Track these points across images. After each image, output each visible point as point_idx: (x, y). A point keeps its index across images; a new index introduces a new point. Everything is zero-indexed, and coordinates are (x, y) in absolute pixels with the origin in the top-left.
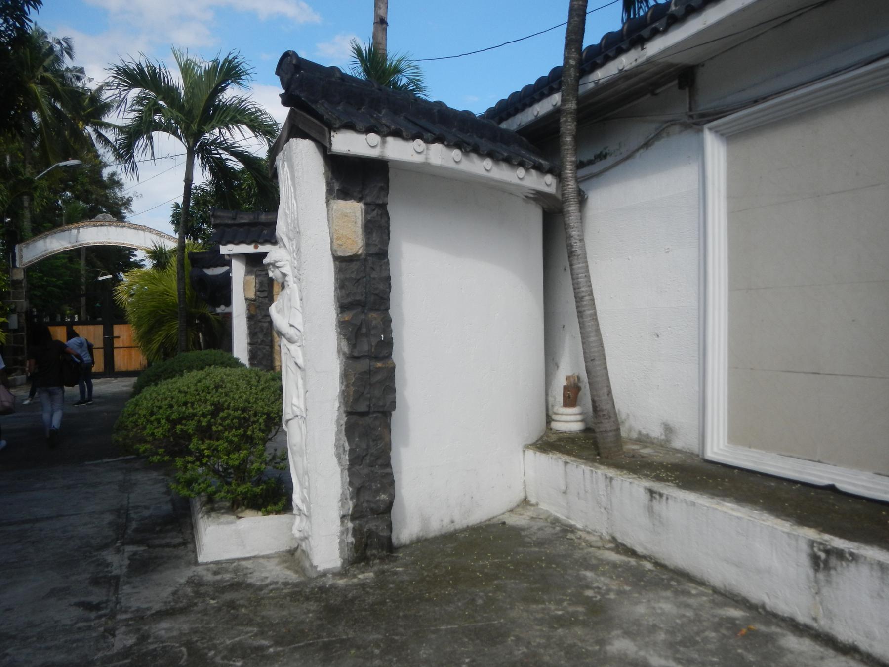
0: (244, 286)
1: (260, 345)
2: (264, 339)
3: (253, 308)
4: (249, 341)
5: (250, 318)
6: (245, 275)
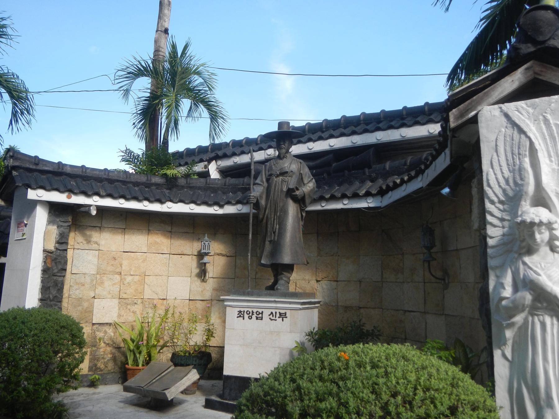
0: (44, 236)
1: (51, 301)
2: (57, 295)
3: (49, 261)
4: (40, 296)
5: (45, 271)
6: (47, 225)
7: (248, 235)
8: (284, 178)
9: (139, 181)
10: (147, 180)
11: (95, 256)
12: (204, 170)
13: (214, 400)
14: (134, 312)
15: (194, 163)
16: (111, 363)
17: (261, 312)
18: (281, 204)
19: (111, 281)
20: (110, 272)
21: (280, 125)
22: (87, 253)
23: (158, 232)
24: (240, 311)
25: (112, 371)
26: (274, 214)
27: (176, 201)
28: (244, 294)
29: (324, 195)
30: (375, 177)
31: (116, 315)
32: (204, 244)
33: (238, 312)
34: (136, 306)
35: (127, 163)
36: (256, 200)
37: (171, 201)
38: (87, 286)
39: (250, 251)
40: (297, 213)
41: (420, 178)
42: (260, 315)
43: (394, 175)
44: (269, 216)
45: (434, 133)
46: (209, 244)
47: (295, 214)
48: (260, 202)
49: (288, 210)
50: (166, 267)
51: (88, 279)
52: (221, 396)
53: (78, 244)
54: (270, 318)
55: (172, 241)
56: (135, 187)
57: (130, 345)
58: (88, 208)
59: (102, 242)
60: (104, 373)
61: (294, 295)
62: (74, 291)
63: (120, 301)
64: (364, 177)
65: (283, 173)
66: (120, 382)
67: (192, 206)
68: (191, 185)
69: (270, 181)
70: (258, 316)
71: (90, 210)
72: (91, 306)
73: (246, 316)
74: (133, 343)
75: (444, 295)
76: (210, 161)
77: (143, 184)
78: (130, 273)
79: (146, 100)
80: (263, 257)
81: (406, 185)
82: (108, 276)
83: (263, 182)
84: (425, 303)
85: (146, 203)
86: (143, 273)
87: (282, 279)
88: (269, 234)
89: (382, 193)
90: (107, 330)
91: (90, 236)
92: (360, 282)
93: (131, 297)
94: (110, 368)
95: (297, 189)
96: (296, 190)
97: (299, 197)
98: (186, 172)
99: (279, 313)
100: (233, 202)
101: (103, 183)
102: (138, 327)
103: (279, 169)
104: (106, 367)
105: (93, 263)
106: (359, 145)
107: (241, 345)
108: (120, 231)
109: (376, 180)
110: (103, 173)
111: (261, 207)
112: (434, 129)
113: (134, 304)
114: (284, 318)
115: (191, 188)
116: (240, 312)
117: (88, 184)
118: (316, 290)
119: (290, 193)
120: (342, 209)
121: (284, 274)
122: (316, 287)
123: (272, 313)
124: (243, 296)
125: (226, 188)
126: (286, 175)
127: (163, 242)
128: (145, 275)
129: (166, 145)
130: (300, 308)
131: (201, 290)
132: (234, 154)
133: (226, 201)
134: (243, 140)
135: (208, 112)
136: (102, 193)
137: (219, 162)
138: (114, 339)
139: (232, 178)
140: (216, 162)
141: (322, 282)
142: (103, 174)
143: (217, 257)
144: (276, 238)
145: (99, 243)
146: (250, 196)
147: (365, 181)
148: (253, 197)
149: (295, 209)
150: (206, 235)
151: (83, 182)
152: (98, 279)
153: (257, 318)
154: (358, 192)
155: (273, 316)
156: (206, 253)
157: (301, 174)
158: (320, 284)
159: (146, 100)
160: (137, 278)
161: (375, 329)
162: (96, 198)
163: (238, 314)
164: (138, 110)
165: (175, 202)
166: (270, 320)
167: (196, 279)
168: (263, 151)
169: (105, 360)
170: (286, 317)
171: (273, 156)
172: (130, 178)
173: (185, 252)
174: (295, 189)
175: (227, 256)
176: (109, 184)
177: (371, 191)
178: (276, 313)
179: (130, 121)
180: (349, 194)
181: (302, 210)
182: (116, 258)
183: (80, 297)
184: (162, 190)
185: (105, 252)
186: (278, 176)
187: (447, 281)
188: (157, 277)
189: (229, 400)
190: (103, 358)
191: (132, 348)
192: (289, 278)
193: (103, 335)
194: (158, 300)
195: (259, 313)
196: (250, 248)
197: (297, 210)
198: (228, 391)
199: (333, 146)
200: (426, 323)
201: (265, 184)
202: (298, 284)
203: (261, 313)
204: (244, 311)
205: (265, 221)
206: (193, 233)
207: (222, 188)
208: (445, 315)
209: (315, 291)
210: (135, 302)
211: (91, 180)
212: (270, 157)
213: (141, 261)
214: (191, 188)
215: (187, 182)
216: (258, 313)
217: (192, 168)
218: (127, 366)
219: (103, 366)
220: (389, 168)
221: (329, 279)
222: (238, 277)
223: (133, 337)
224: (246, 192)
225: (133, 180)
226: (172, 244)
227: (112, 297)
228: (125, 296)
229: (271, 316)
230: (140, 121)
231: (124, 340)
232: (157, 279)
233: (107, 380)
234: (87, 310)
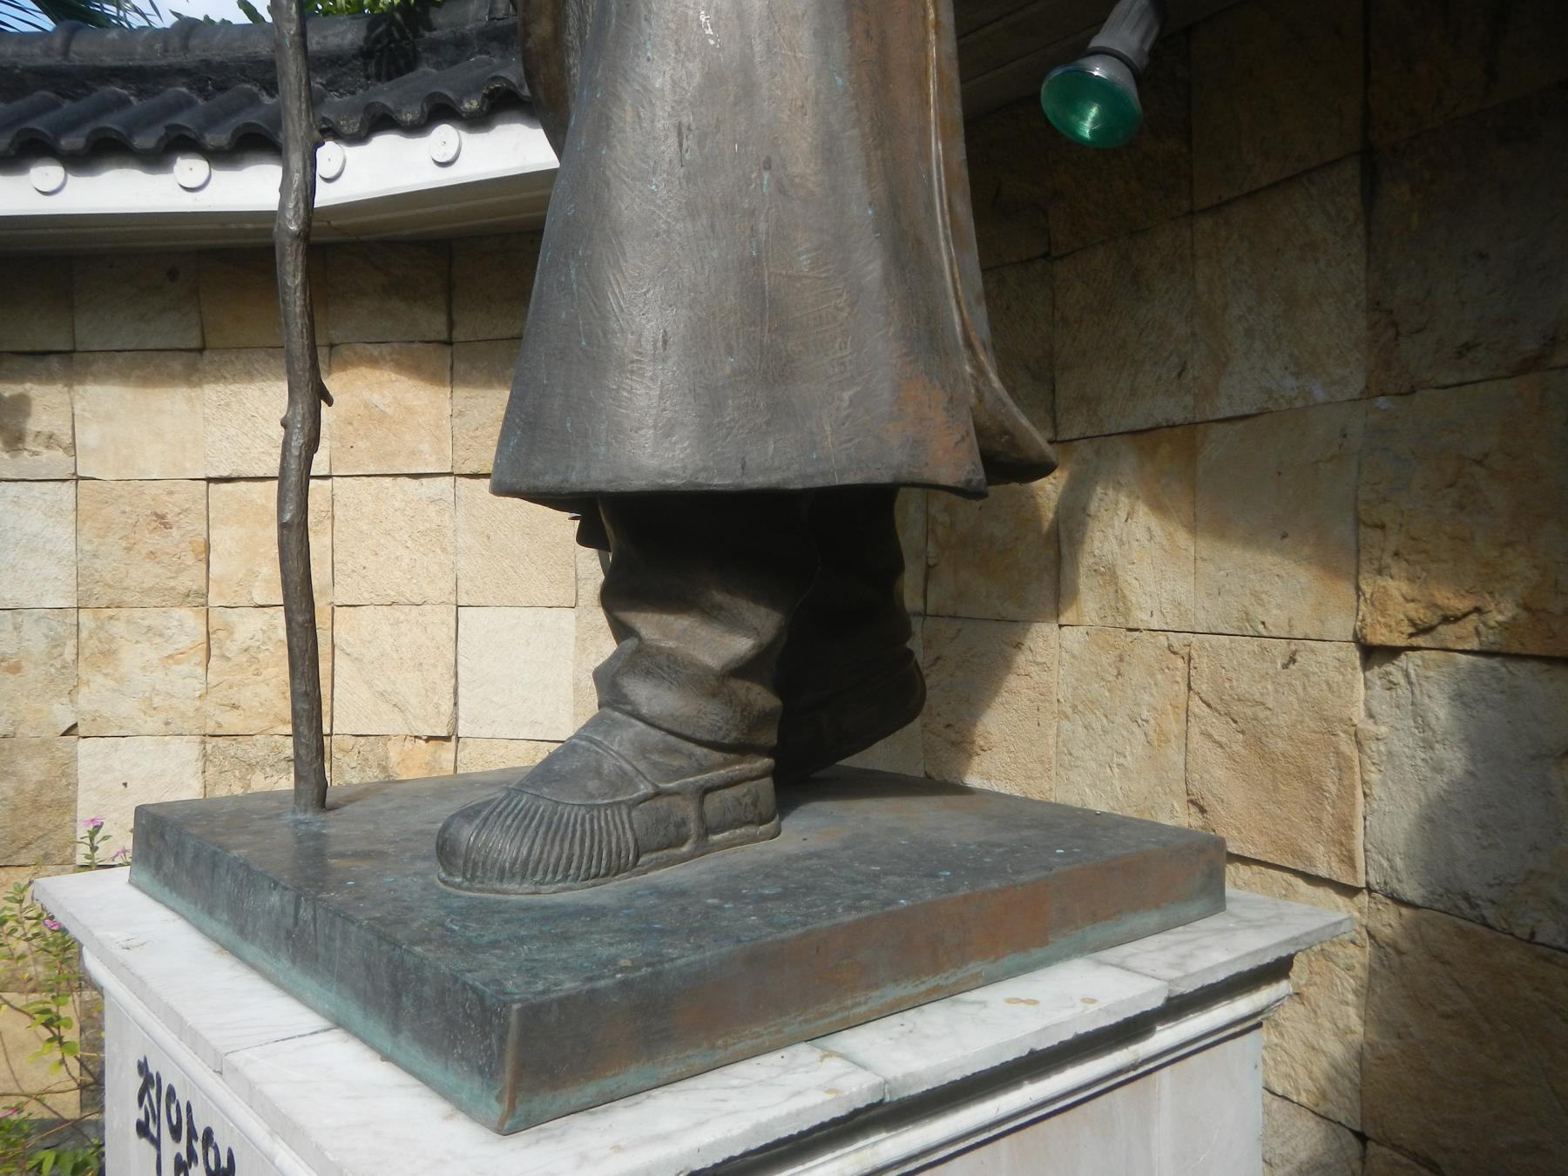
19: (157, 640)
22: (16, 501)
23: (375, 350)
38: (30, 672)
50: (444, 550)
51: (35, 639)
55: (462, 393)
67: (445, 136)
72: (64, 774)
82: (138, 613)
93: (265, 724)
108: (177, 365)
122: (1358, 715)
127: (410, 410)
141: (1409, 661)
152: (84, 635)
158: (1391, 686)
182: (170, 518)
185: (105, 484)
188: (397, 613)
194: (408, 745)
202: (1202, 663)
221: (1490, 638)
227: (163, 729)
228: (232, 722)
232: (398, 622)
234: (45, 799)
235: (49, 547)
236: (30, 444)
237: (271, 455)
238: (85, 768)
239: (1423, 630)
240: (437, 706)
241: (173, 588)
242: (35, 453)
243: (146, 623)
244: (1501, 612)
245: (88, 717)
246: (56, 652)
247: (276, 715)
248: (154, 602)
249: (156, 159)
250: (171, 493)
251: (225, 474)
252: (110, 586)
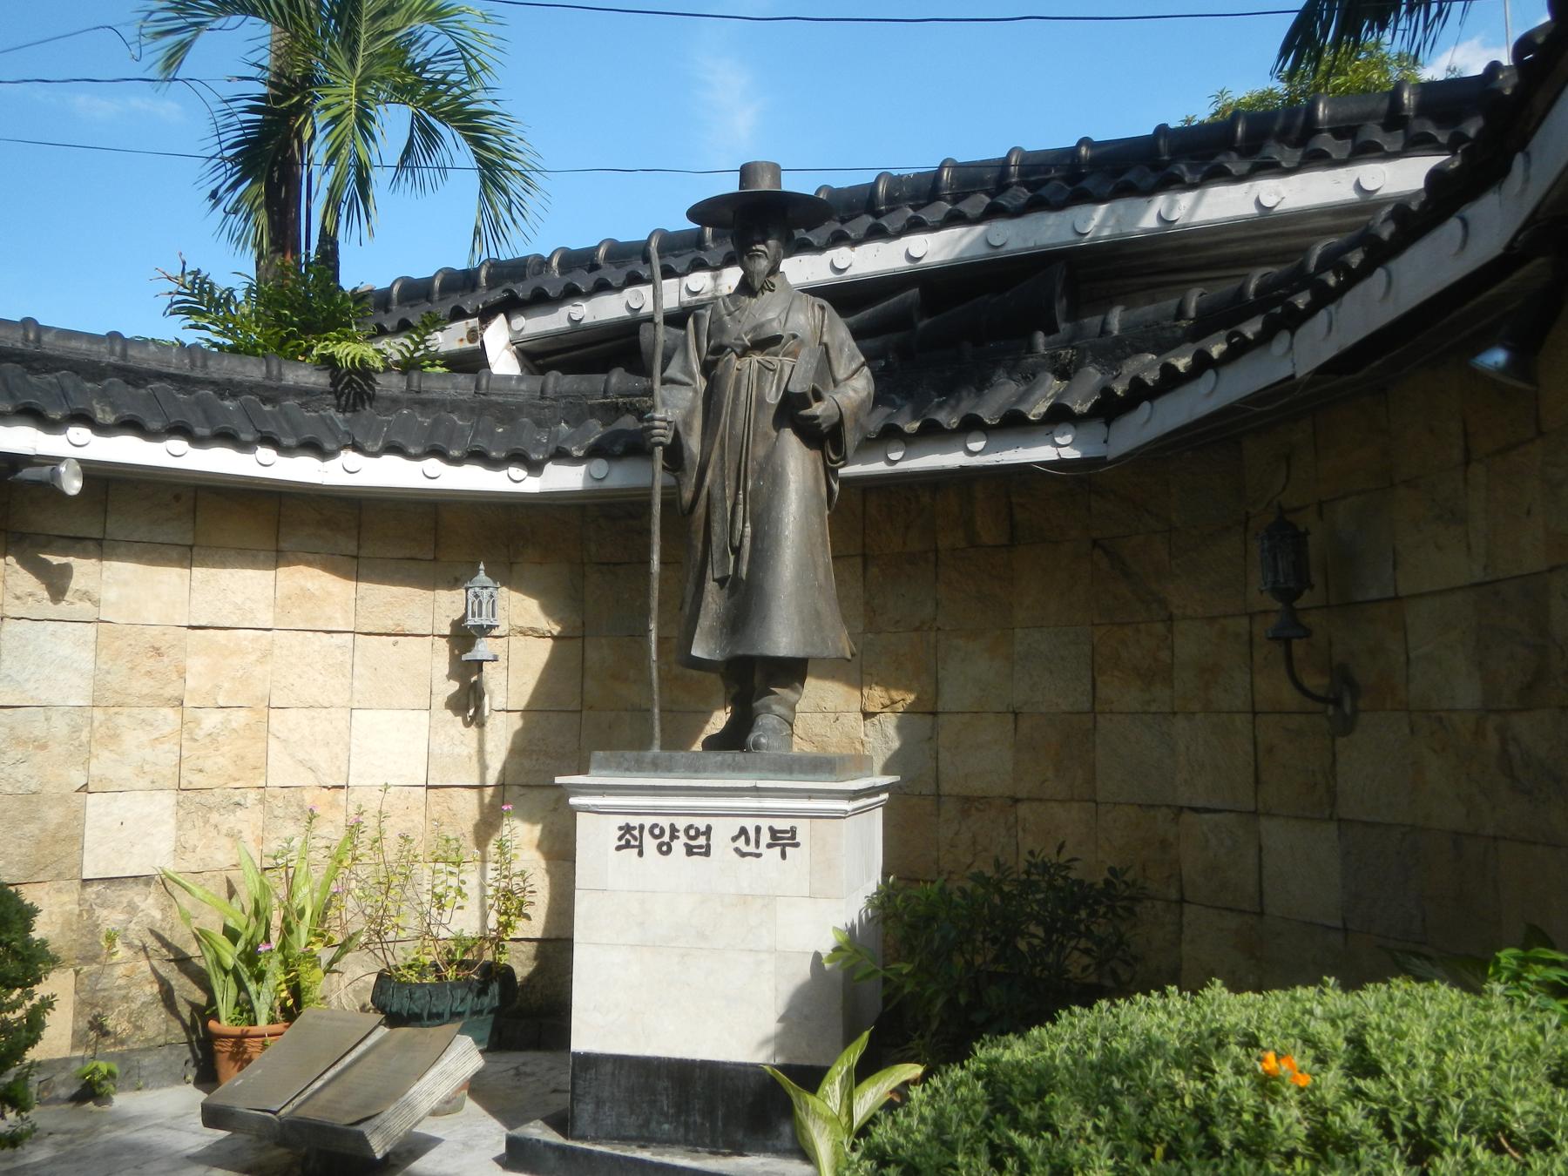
7: (647, 562)
8: (768, 358)
9: (238, 378)
10: (268, 376)
11: (85, 643)
12: (467, 345)
13: (538, 1141)
14: (234, 836)
15: (436, 323)
16: (156, 1012)
17: (703, 829)
18: (760, 451)
20: (142, 697)
21: (746, 172)
22: (53, 634)
23: (310, 557)
24: (627, 825)
25: (161, 1040)
26: (733, 484)
27: (376, 449)
28: (639, 767)
29: (899, 423)
30: (1071, 361)
31: (167, 846)
32: (477, 596)
33: (621, 828)
34: (239, 813)
35: (192, 322)
36: (671, 434)
37: (357, 448)
39: (654, 614)
40: (817, 480)
41: (1281, 343)
42: (702, 840)
43: (1143, 351)
44: (717, 493)
45: (1276, 209)
46: (492, 596)
47: (810, 483)
48: (684, 442)
49: (784, 468)
50: (344, 676)
51: (60, 726)
52: (561, 1123)
53: (17, 602)
54: (737, 850)
55: (363, 586)
56: (222, 397)
57: (223, 953)
58: (48, 468)
59: (110, 594)
60: (131, 1051)
61: (821, 765)
62: (8, 770)
63: (181, 798)
64: (1030, 360)
65: (766, 343)
66: (190, 1077)
67: (433, 465)
68: (424, 396)
69: (719, 370)
70: (692, 843)
71: (56, 475)
73: (650, 844)
74: (235, 944)
75: (1334, 755)
76: (486, 316)
77: (253, 388)
78: (215, 699)
79: (252, 110)
80: (696, 636)
81: (1217, 374)
82: (136, 710)
83: (692, 377)
84: (1257, 781)
85: (265, 454)
86: (262, 700)
87: (768, 710)
88: (716, 556)
89: (1109, 409)
90: (137, 899)
91: (66, 571)
92: (1016, 714)
94: (150, 1032)
95: (818, 397)
96: (812, 401)
97: (824, 426)
98: (404, 350)
99: (771, 829)
100: (576, 453)
101: (106, 383)
102: (248, 888)
103: (747, 327)
104: (140, 1028)
105: (76, 669)
106: (1012, 252)
107: (632, 945)
108: (174, 554)
109: (1076, 371)
110: (103, 348)
111: (687, 462)
112: (1277, 194)
113: (232, 807)
114: (788, 849)
115: (425, 404)
116: (627, 829)
117: (50, 383)
118: (863, 745)
119: (792, 411)
120: (963, 471)
121: (774, 693)
123: (743, 831)
124: (635, 774)
125: (548, 407)
126: (773, 349)
127: (329, 594)
128: (269, 706)
129: (332, 264)
130: (846, 812)
131: (465, 753)
132: (571, 293)
133: (552, 448)
134: (597, 248)
135: (474, 152)
136: (105, 416)
137: (520, 322)
138: (164, 930)
139: (565, 372)
140: (508, 320)
142: (102, 350)
143: (518, 642)
144: (744, 569)
145: (97, 596)
146: (652, 419)
147: (1034, 376)
148: (664, 424)
149: (810, 467)
150: (482, 566)
151: (29, 377)
152: (96, 724)
153: (690, 851)
154: (1023, 408)
155: (747, 842)
156: (482, 626)
157: (826, 346)
159: (252, 110)
160: (239, 718)
161: (1117, 878)
162: (79, 433)
163: (620, 838)
164: (224, 145)
165: (370, 450)
166: (736, 856)
167: (449, 713)
168: (674, 281)
169: (134, 1006)
170: (797, 845)
171: (709, 295)
172: (205, 366)
173: (409, 626)
174: (810, 395)
175: (553, 637)
176: (130, 389)
177: (1069, 404)
178: (758, 829)
179: (199, 185)
180: (988, 414)
181: (830, 472)
182: (163, 650)
183: (33, 788)
184: (322, 412)
185: (119, 627)
186: (744, 352)
187: (1348, 708)
188: (312, 713)
189: (596, 1139)
190: (125, 998)
191: (229, 962)
192: (793, 709)
193: (122, 917)
194: (317, 792)
195: (698, 833)
196: (654, 604)
197: (816, 469)
198: (590, 1108)
199: (919, 259)
200: (1261, 849)
201: (701, 383)
203: (703, 834)
204: (642, 827)
205: (700, 510)
206: (435, 559)
207: (532, 405)
208: (1340, 820)
209: (859, 746)
210: (237, 799)
211: (57, 370)
212: (698, 300)
213: (253, 658)
214: (425, 404)
215: (409, 385)
216: (692, 833)
217: (427, 337)
218: (212, 1024)
219: (125, 1025)
220: (1123, 329)
222: (591, 708)
223: (231, 923)
224: (618, 418)
225: (216, 376)
226: (362, 598)
227: (150, 786)
228: (198, 780)
229: (741, 843)
230: (234, 187)
231: (201, 936)
232: (313, 718)
233: (143, 1073)
234: (62, 835)
235: (75, 665)
236: (69, 596)
237: (234, 614)
238: (91, 813)
239: (885, 707)
240: (339, 768)
241: (161, 695)
242: (72, 603)
243: (142, 717)
244: (911, 698)
245: (96, 779)
246: (75, 735)
247: (229, 776)
248: (148, 703)
249: (244, 446)
250: (165, 634)
251: (203, 624)
252: (117, 692)
